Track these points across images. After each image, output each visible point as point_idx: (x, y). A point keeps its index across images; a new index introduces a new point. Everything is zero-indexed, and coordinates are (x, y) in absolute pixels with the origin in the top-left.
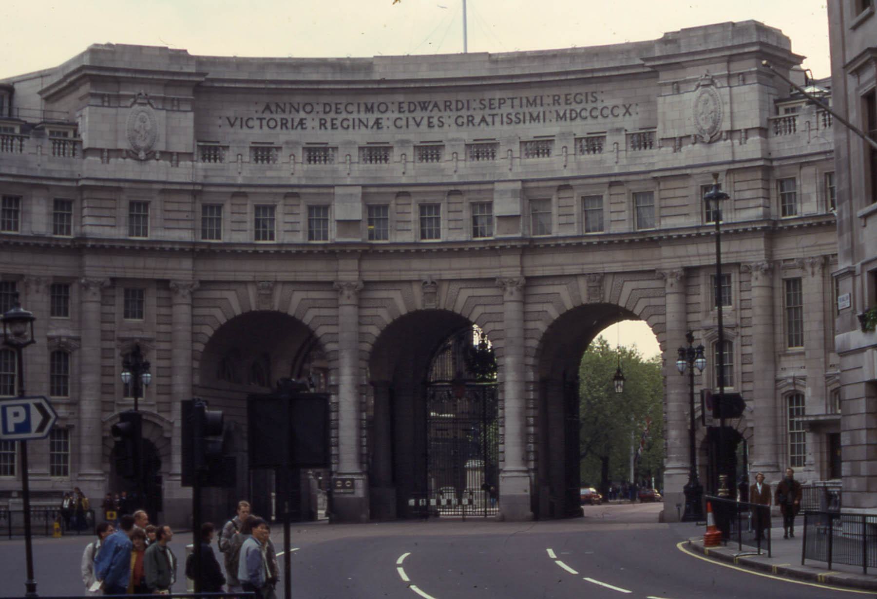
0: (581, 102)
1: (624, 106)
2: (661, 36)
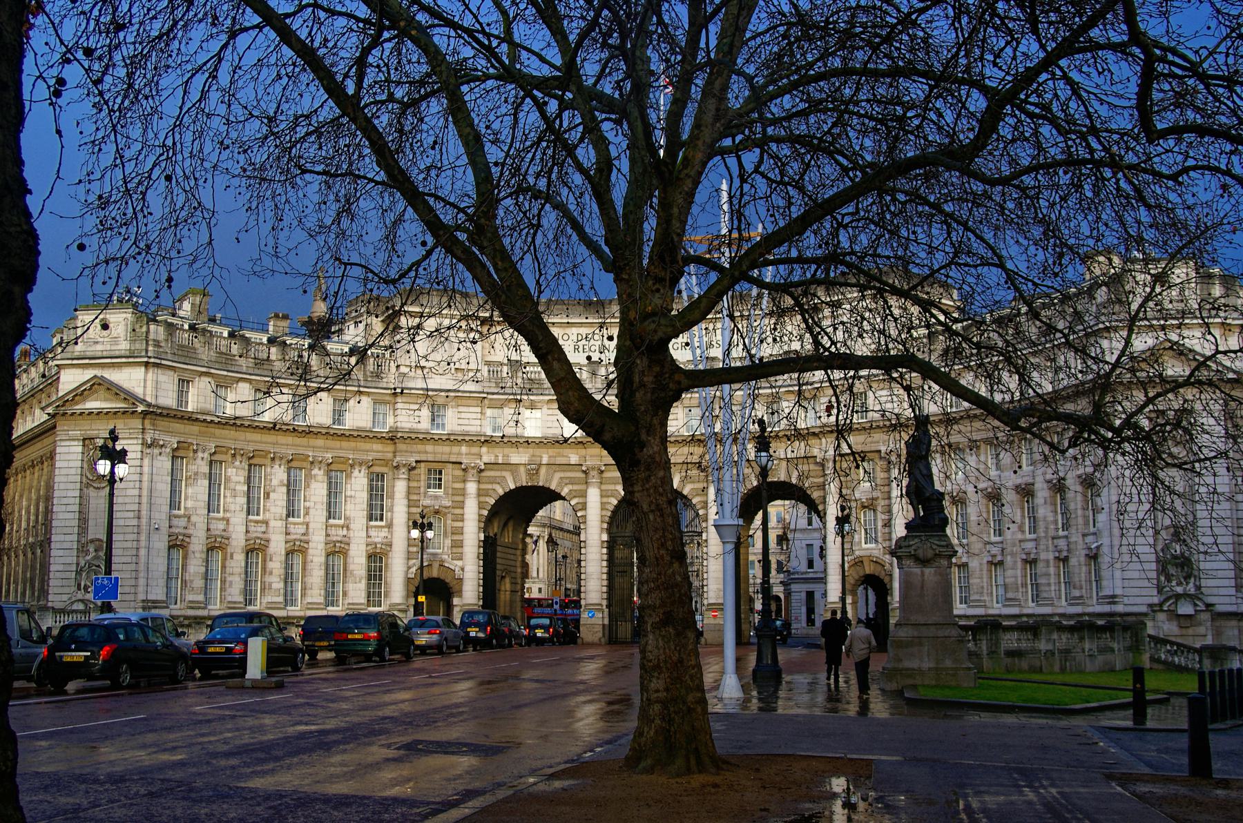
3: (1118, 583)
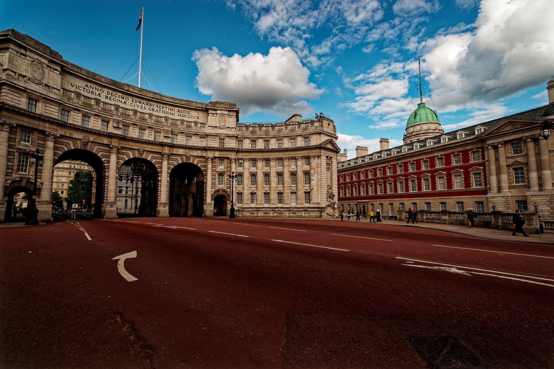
3: (320, 199)
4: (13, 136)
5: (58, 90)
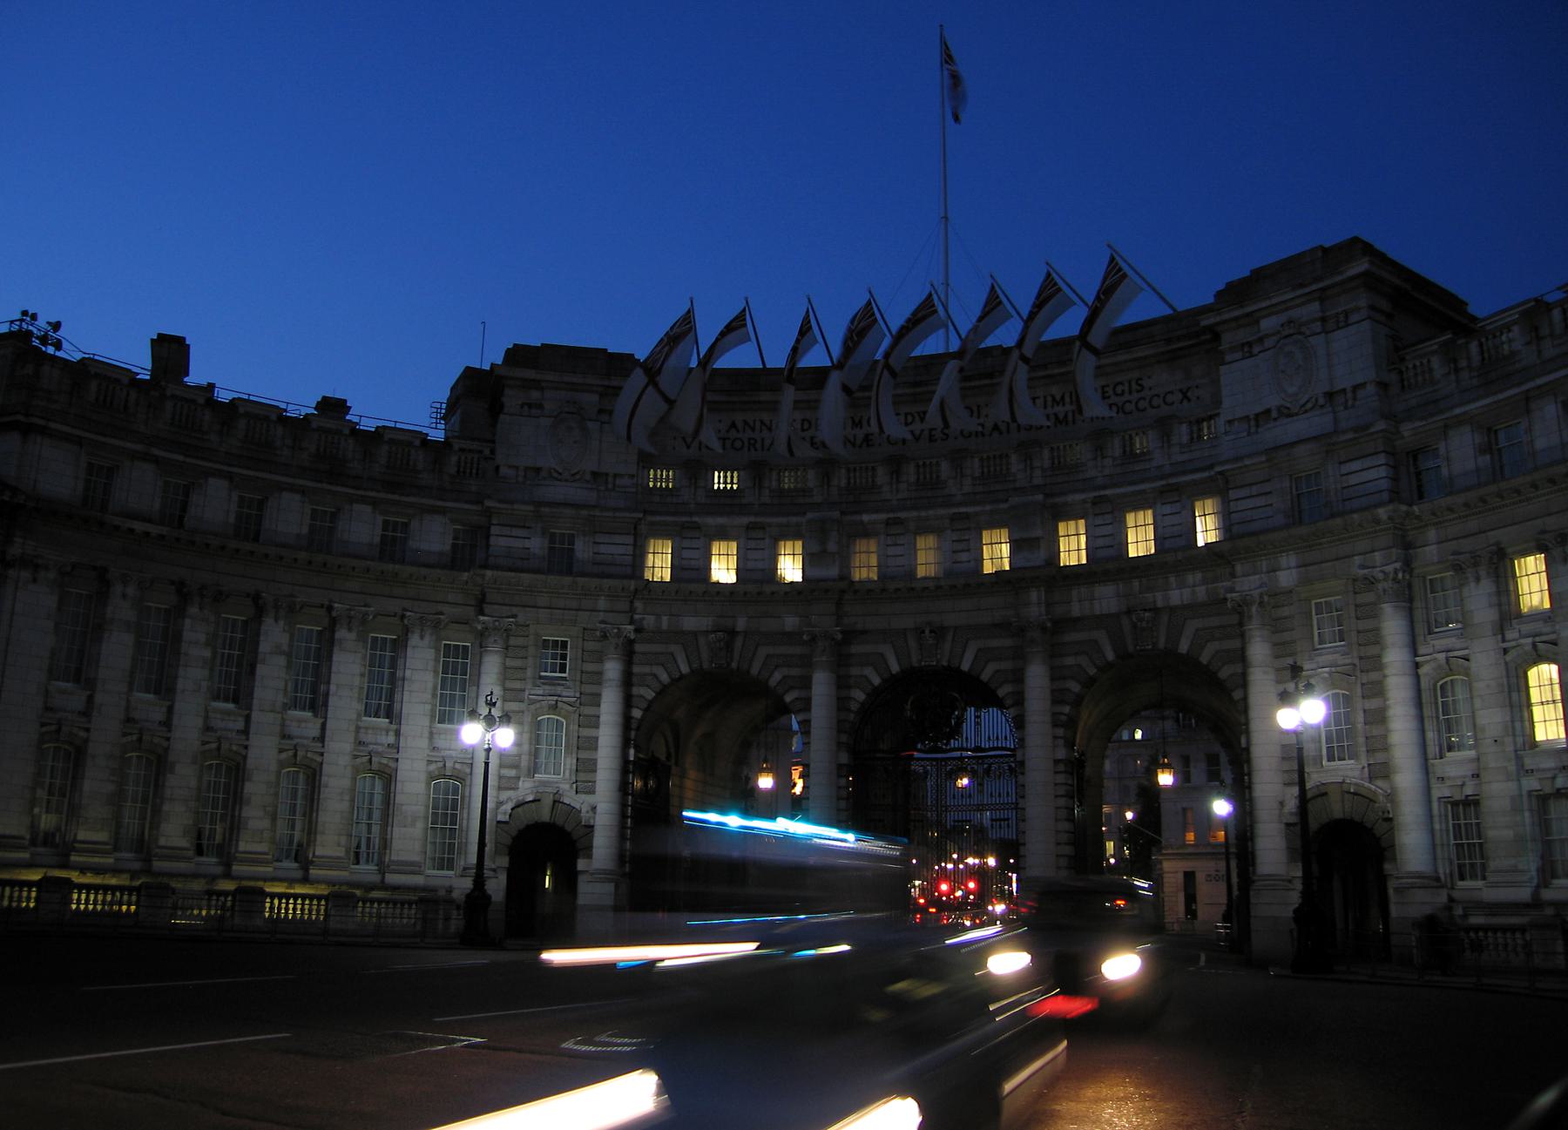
0: (1123, 393)
1: (1181, 391)
2: (1221, 286)
4: (518, 663)
5: (633, 476)
